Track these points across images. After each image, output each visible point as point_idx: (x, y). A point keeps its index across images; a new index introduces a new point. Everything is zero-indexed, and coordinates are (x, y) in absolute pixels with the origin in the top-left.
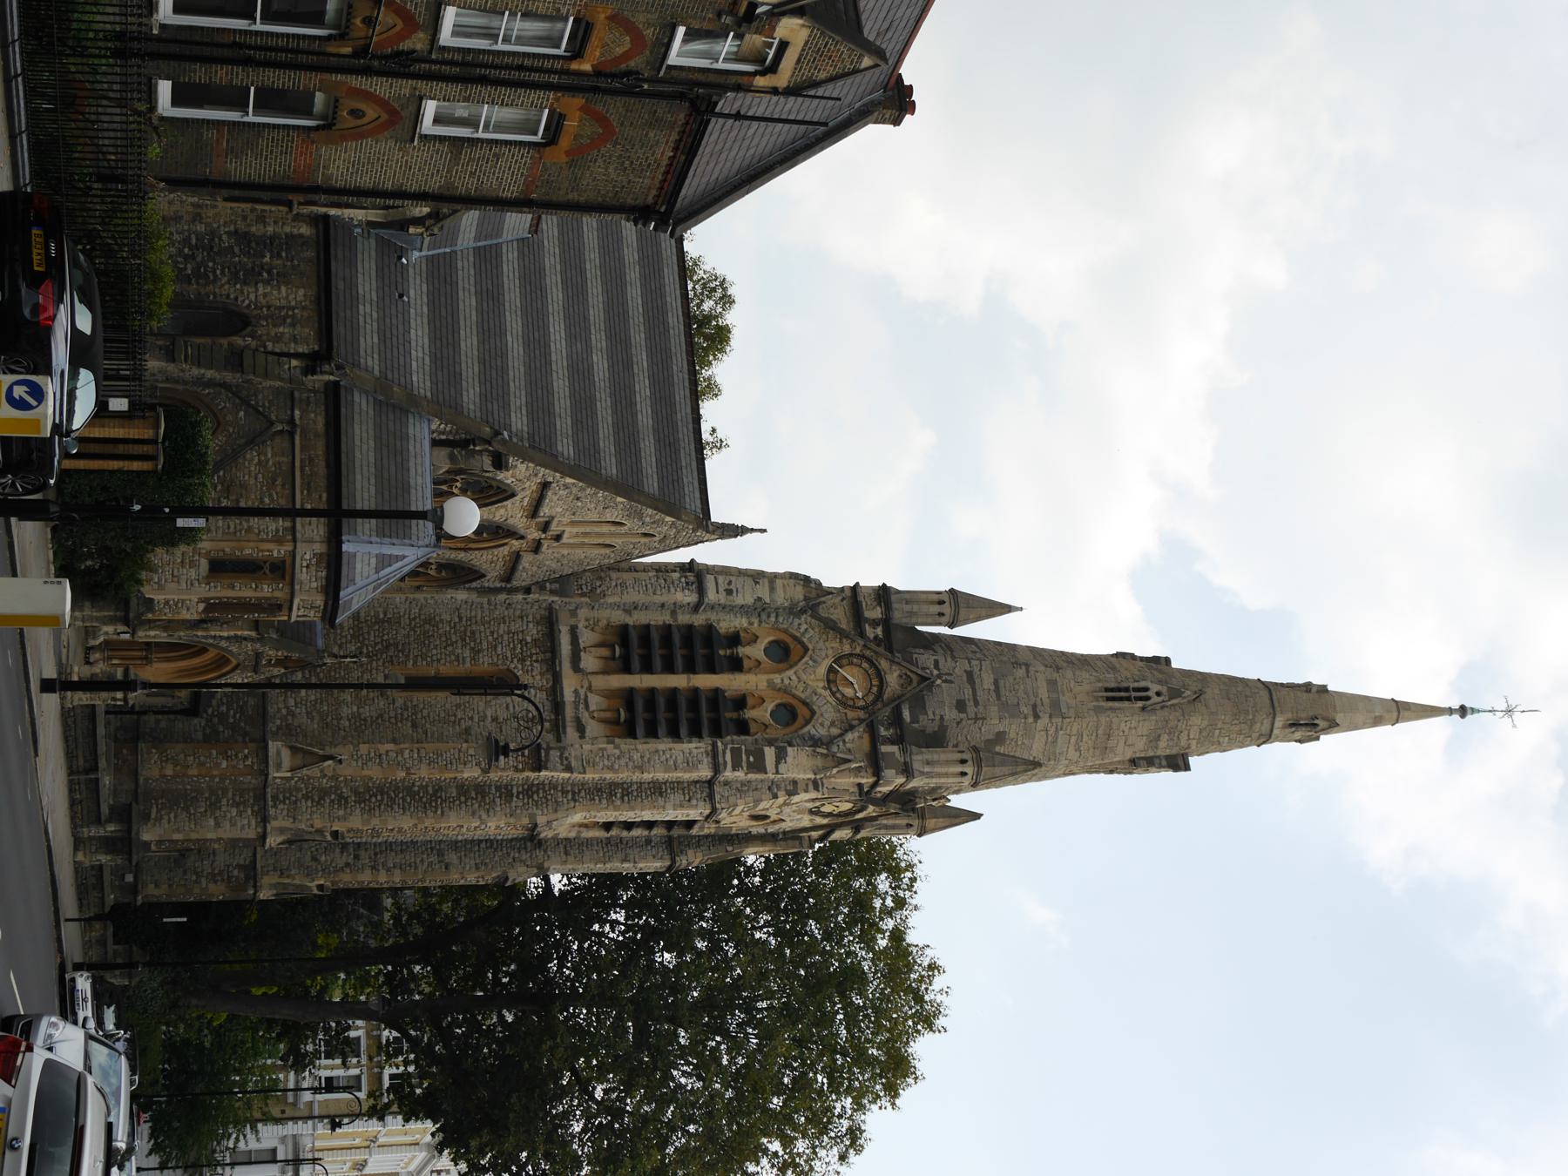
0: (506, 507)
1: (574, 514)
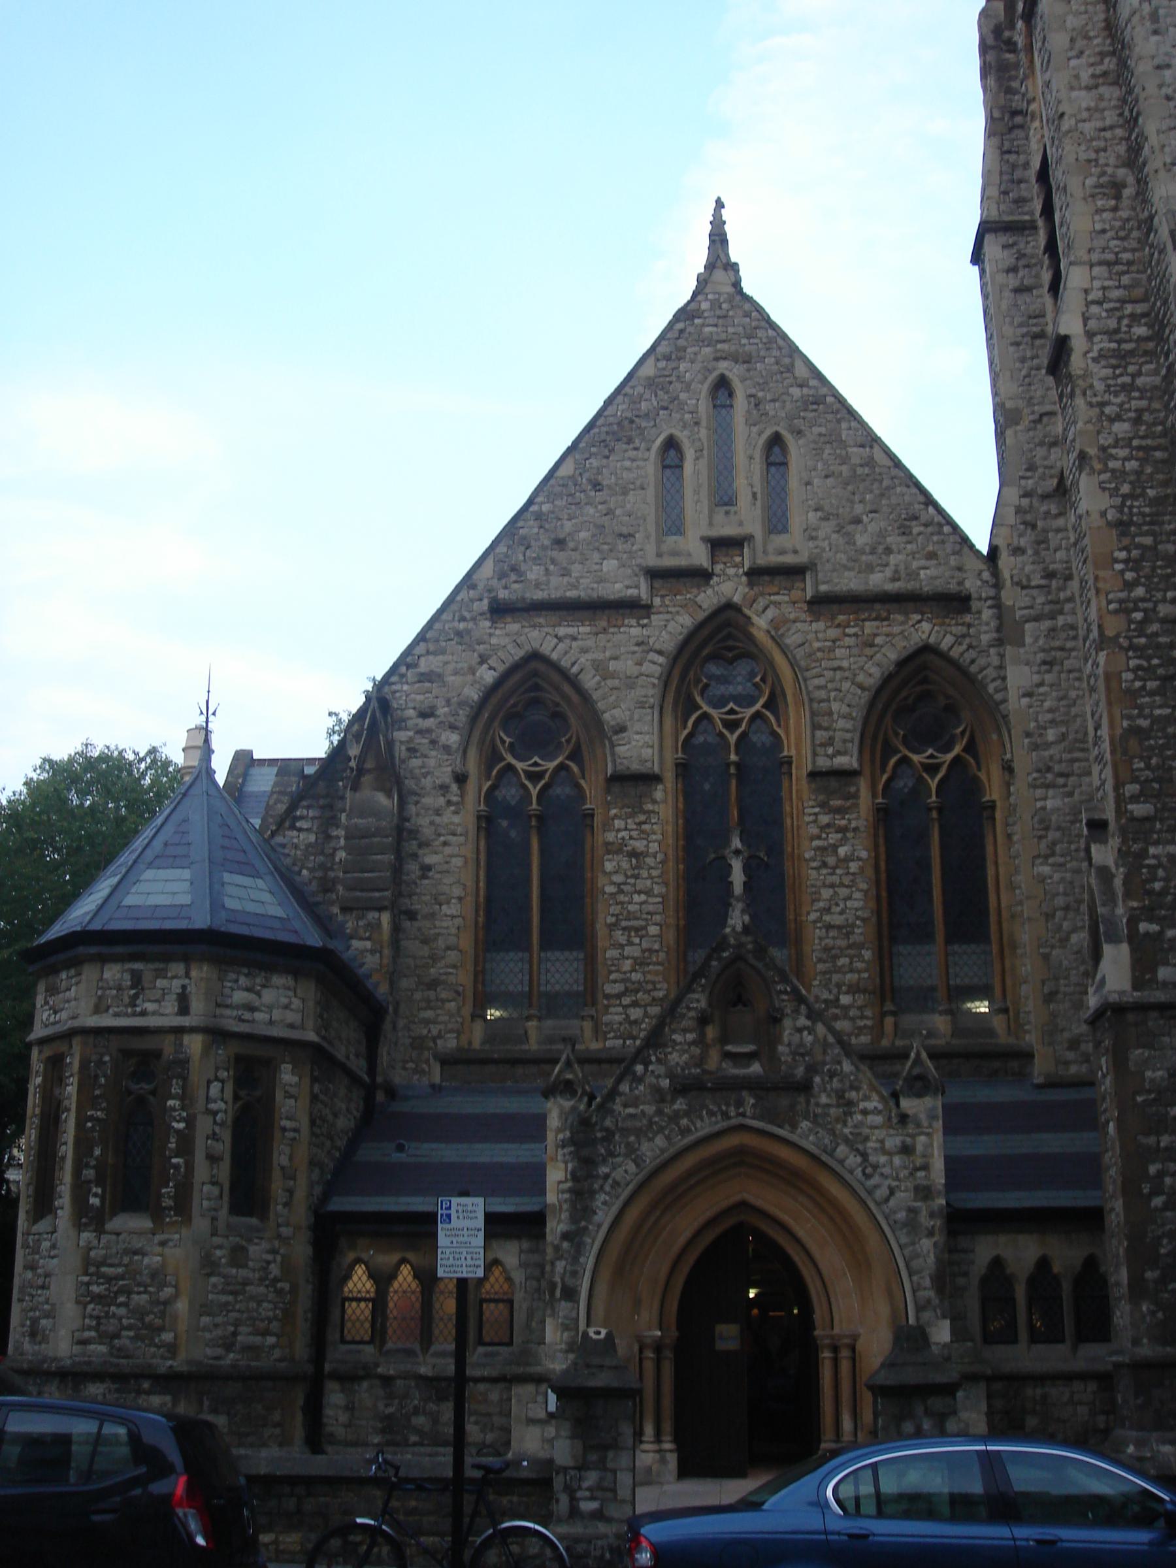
0: (599, 667)
1: (629, 536)
